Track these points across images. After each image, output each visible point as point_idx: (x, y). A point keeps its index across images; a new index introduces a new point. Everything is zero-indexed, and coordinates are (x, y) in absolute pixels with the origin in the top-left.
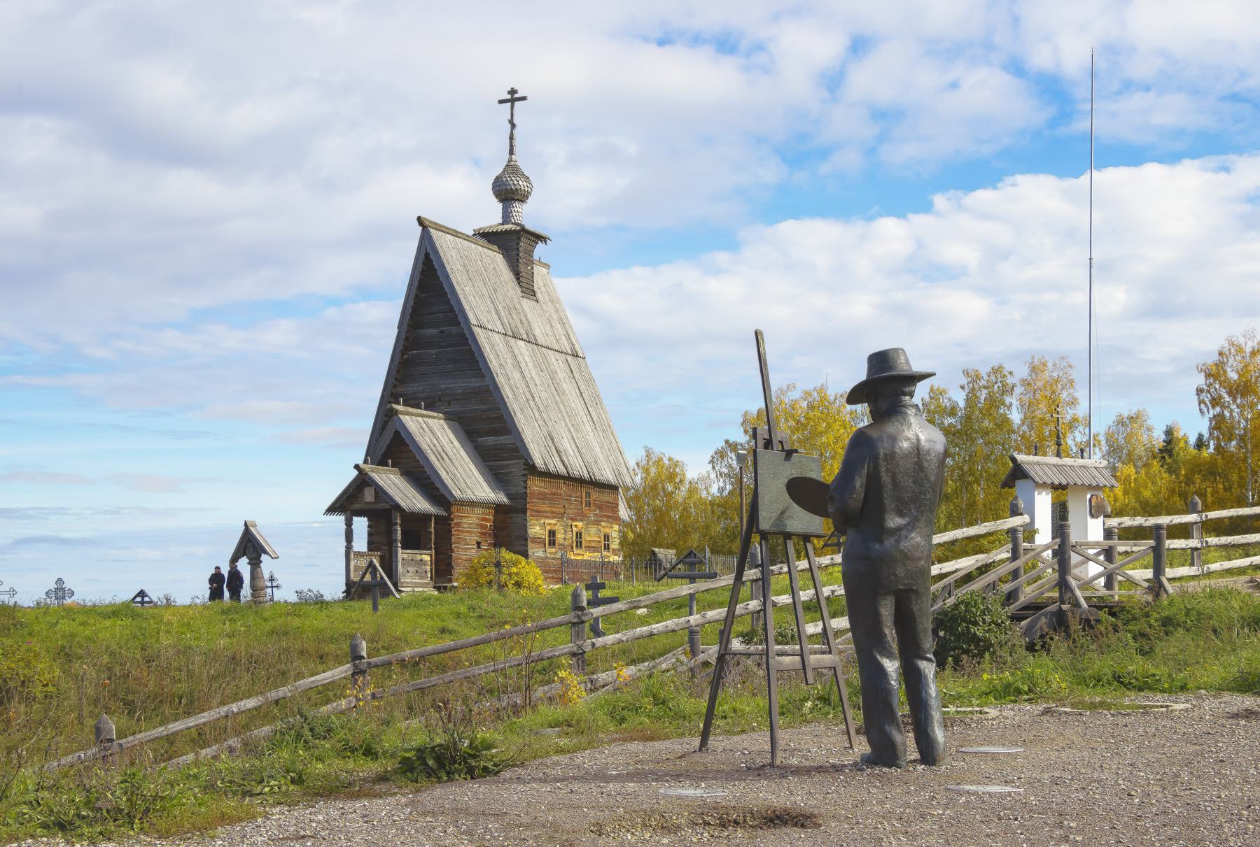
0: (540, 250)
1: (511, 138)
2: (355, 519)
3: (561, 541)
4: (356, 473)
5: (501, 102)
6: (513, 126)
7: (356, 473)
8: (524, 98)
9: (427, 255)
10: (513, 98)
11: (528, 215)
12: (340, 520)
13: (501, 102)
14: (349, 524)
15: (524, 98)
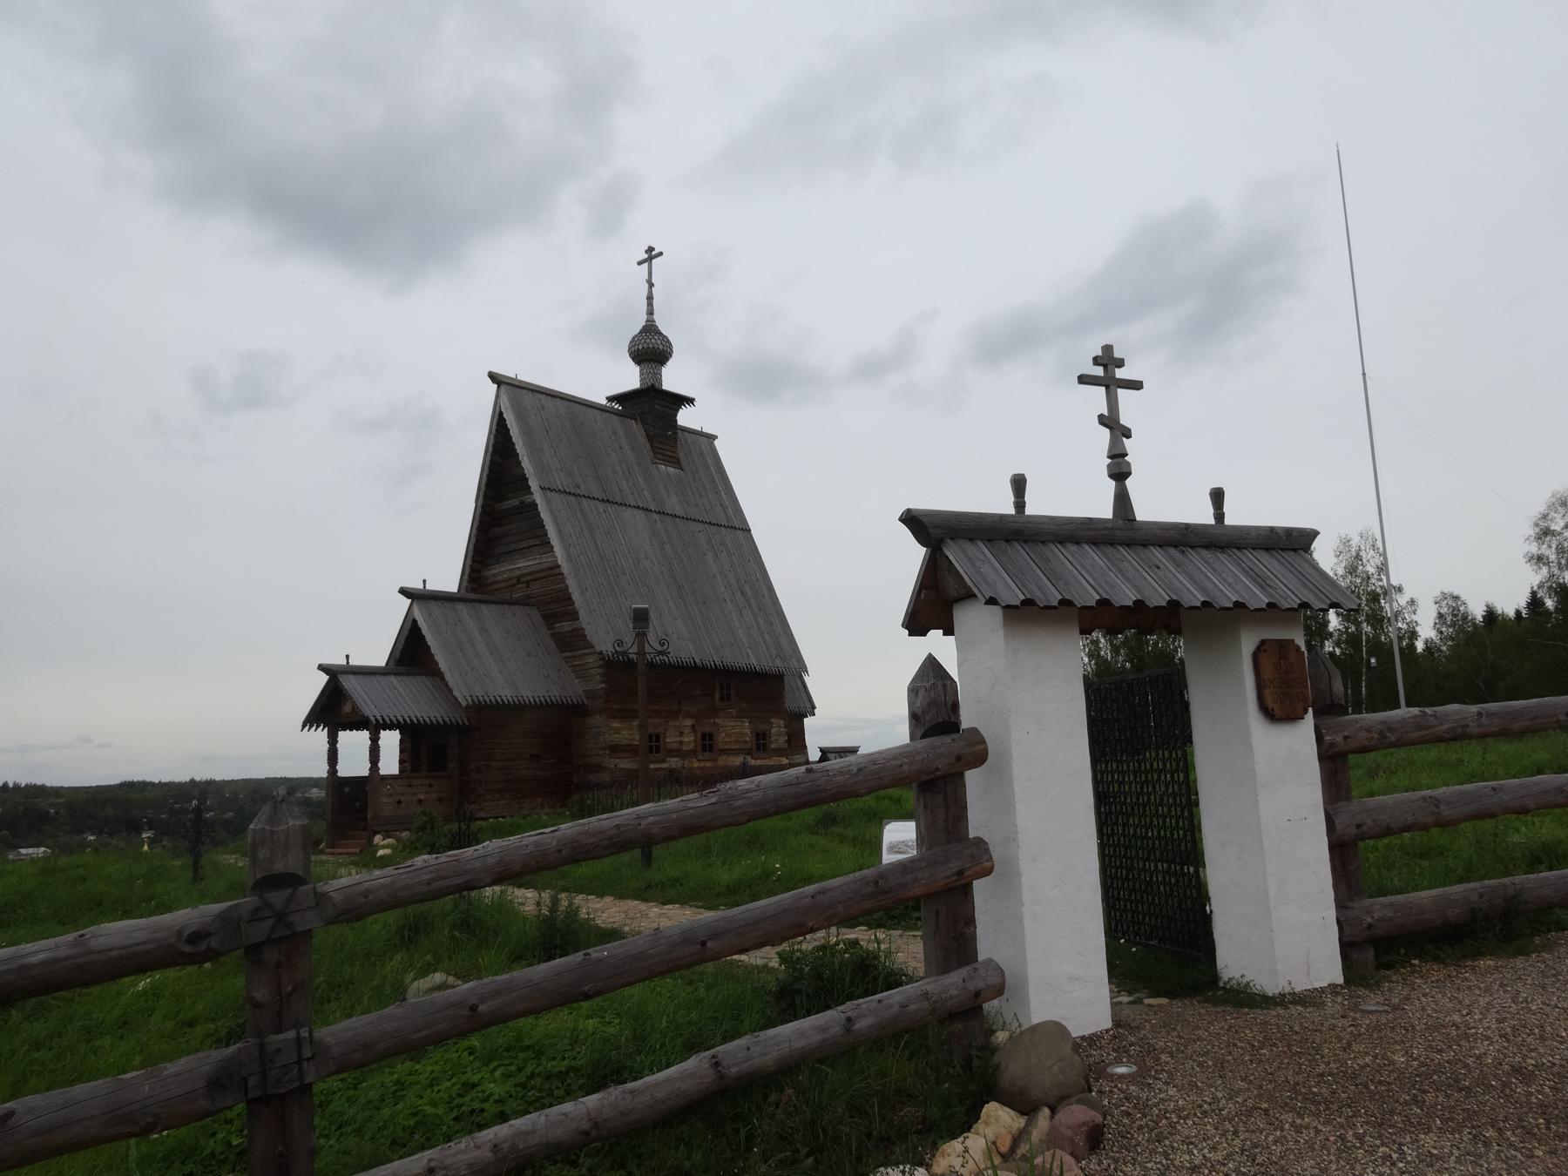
0: (685, 418)
1: (650, 298)
2: (344, 736)
3: (675, 746)
4: (324, 678)
5: (640, 263)
6: (651, 285)
7: (324, 678)
8: (661, 254)
9: (501, 414)
10: (651, 255)
11: (672, 379)
12: (320, 736)
13: (640, 263)
14: (333, 741)
15: (661, 254)
